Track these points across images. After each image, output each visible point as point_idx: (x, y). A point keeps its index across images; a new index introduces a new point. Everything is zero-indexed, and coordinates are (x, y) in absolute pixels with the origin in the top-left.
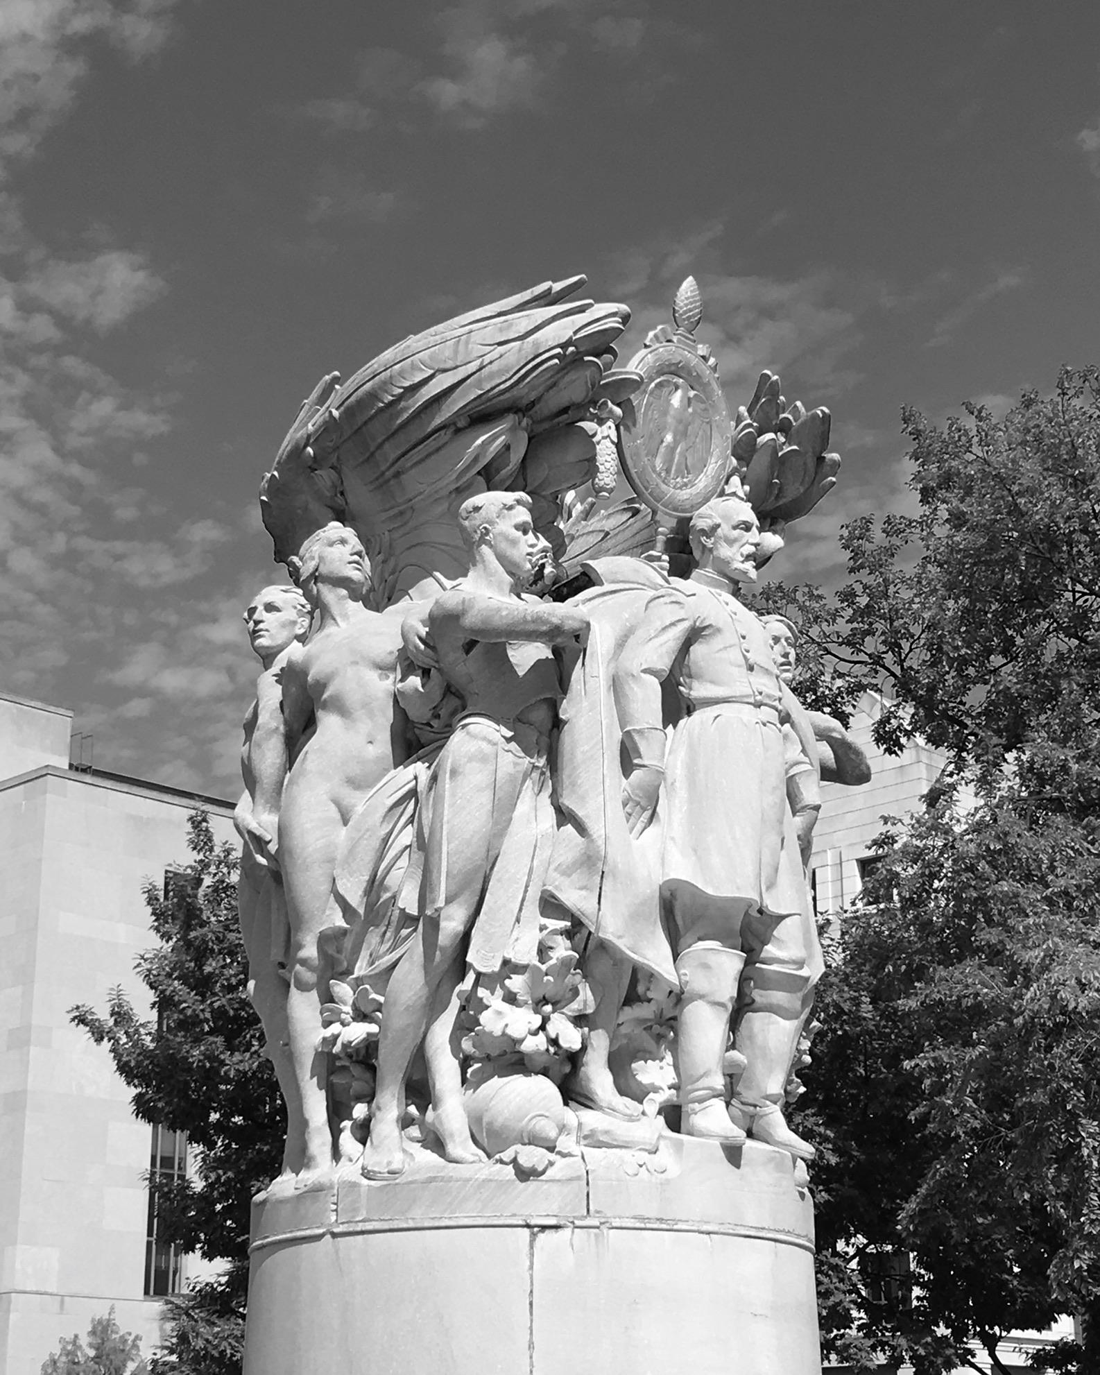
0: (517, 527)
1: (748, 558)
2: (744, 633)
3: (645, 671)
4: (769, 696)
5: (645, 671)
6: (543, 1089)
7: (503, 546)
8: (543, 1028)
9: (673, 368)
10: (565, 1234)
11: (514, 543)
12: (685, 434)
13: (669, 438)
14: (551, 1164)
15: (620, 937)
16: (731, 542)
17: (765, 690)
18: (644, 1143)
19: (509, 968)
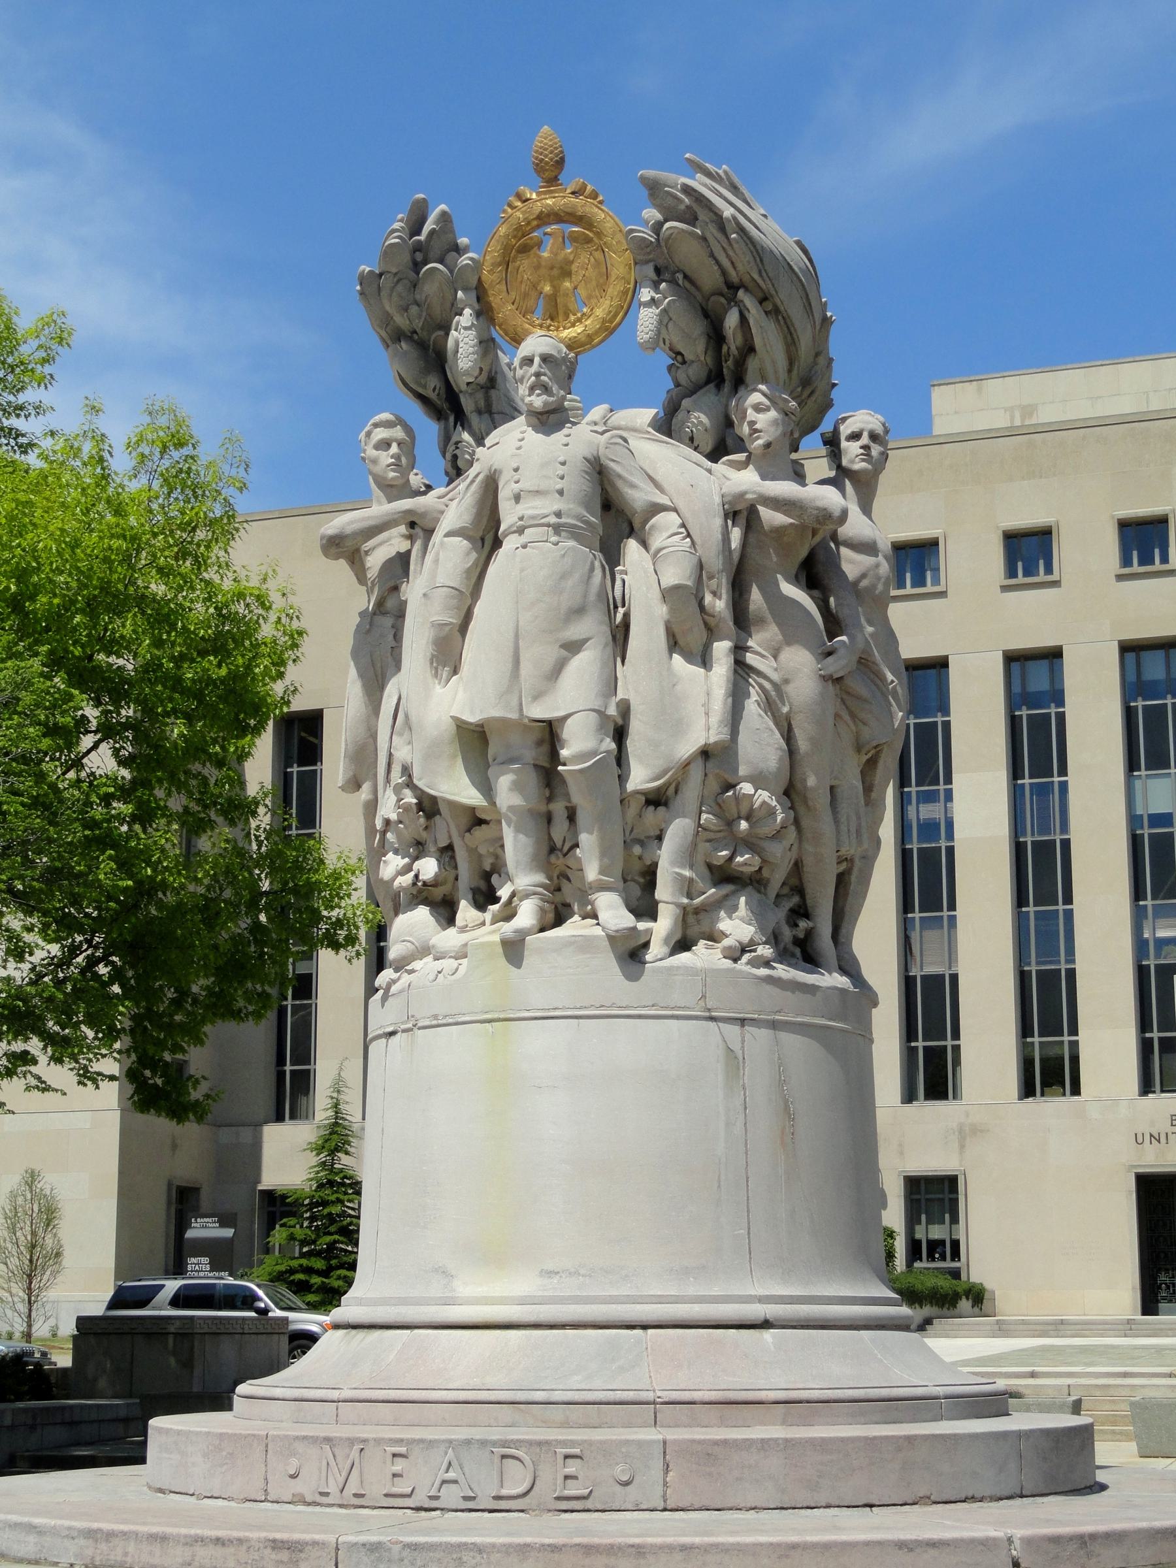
0: (377, 447)
1: (532, 389)
2: (515, 466)
3: (448, 535)
4: (533, 517)
5: (448, 535)
6: (423, 913)
7: (371, 466)
8: (408, 869)
9: (535, 223)
10: (398, 1035)
11: (375, 461)
12: (566, 273)
13: (547, 289)
14: (394, 982)
15: (420, 779)
16: (521, 380)
17: (531, 512)
18: (451, 951)
19: (387, 822)
